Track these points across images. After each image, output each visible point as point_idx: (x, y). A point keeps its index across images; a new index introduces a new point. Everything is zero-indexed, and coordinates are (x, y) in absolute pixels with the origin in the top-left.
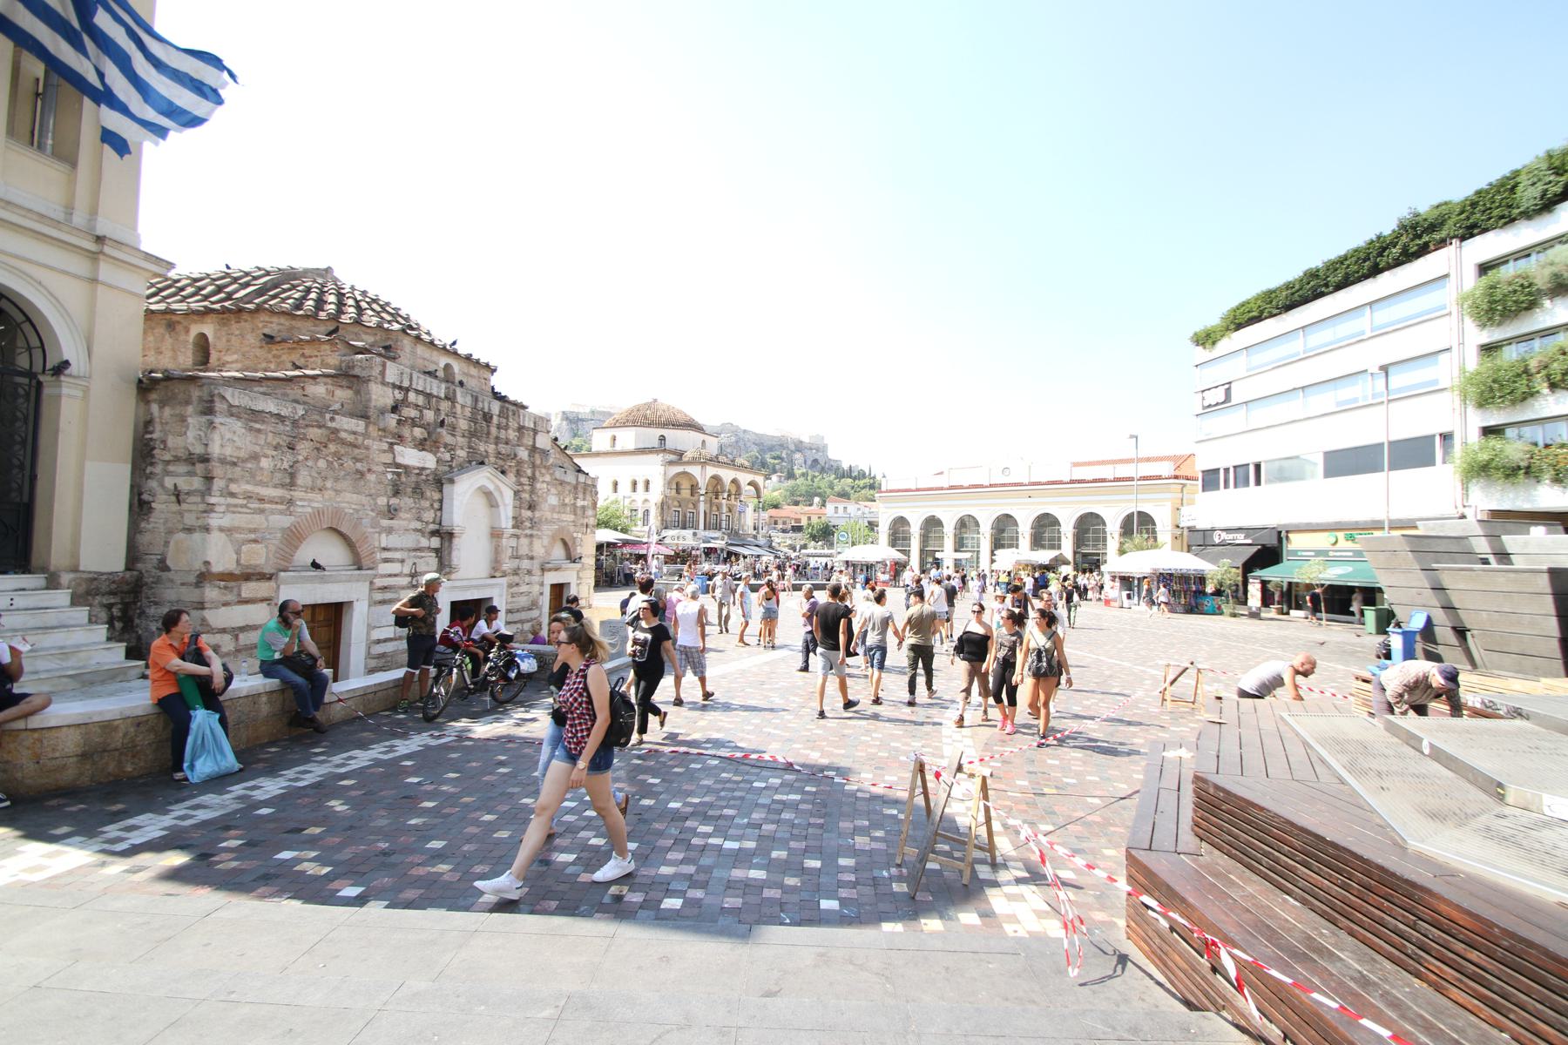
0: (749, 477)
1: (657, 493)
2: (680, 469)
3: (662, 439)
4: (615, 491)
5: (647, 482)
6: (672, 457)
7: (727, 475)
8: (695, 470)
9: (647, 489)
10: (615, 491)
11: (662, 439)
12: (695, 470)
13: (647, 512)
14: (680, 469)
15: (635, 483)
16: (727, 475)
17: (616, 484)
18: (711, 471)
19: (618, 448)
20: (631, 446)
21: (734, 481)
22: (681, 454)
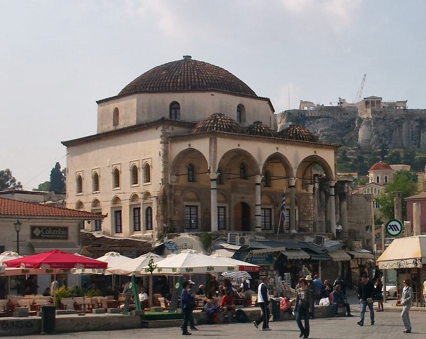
0: (305, 152)
1: (155, 186)
2: (182, 146)
3: (175, 106)
4: (117, 183)
5: (147, 168)
6: (178, 130)
7: (260, 151)
8: (202, 146)
9: (148, 179)
10: (117, 183)
11: (175, 106)
12: (202, 146)
13: (149, 209)
14: (182, 146)
15: (135, 171)
16: (260, 151)
17: (117, 174)
18: (226, 145)
19: (122, 125)
20: (133, 122)
21: (276, 158)
22: (193, 125)
